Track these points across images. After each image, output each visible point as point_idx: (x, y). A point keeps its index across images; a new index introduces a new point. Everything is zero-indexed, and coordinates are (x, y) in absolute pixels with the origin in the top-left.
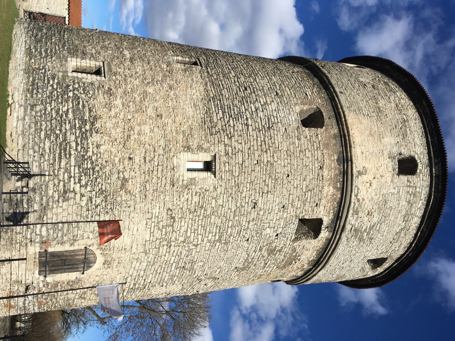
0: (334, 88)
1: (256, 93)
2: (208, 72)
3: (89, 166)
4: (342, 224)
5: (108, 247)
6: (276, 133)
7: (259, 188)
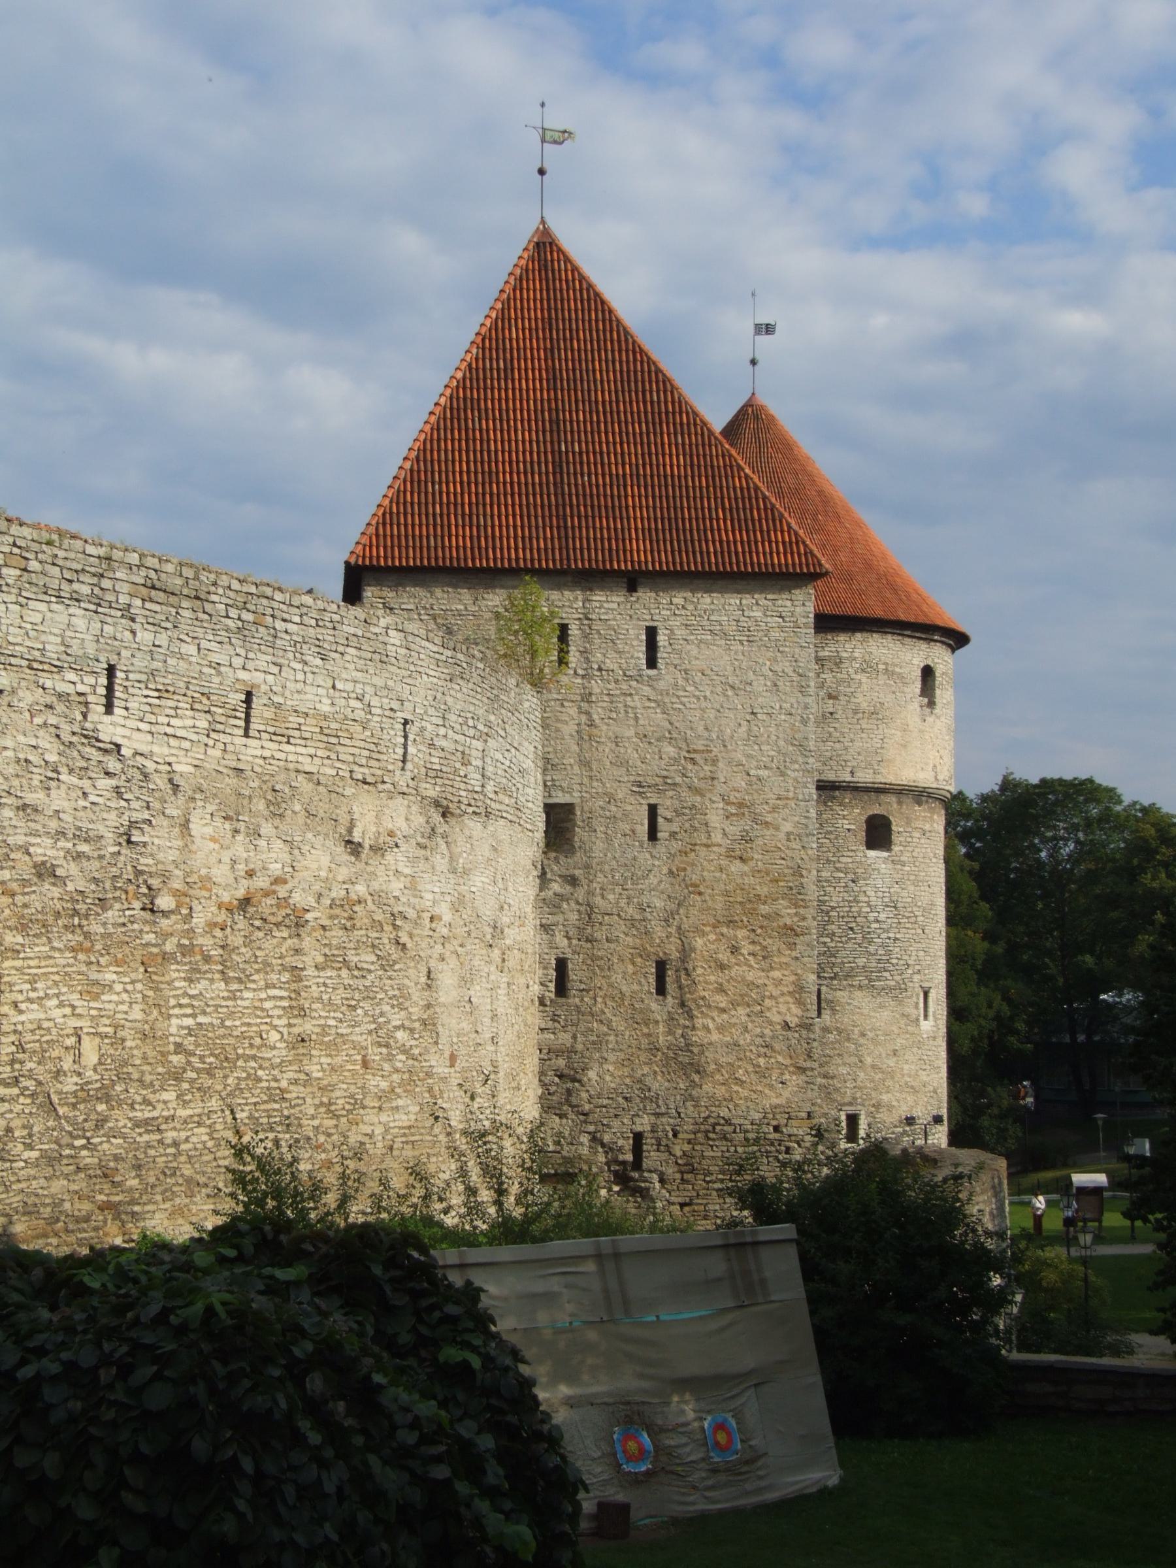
1: (856, 914)
2: (831, 978)
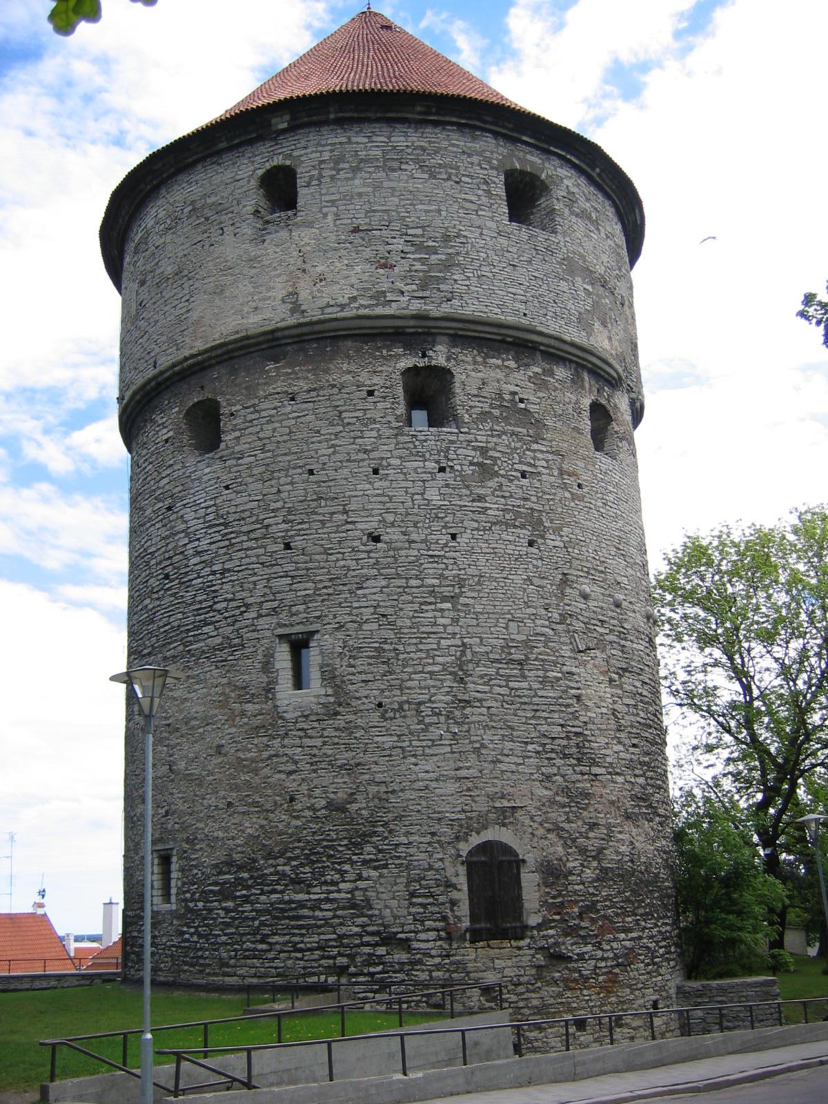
0: (150, 381)
3: (307, 869)
4: (412, 323)
5: (463, 822)
6: (233, 509)
7: (336, 532)
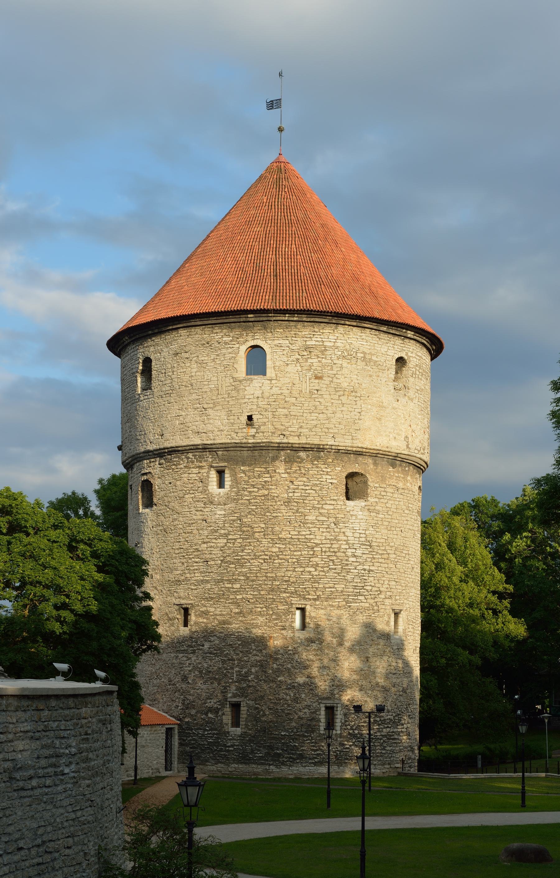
1: (336, 550)
2: (315, 600)
6: (374, 540)
